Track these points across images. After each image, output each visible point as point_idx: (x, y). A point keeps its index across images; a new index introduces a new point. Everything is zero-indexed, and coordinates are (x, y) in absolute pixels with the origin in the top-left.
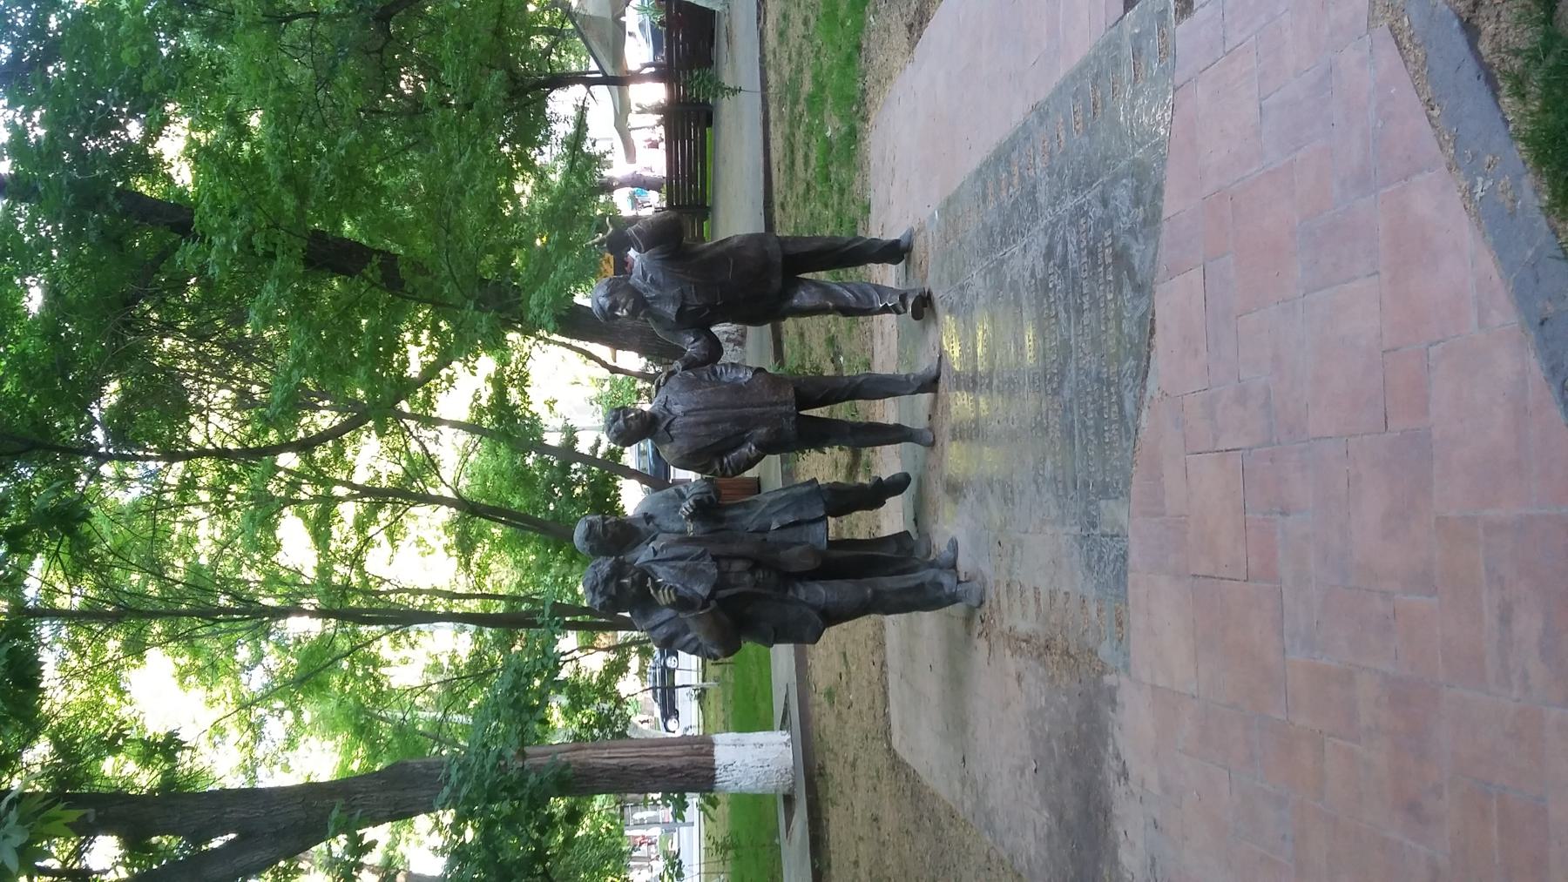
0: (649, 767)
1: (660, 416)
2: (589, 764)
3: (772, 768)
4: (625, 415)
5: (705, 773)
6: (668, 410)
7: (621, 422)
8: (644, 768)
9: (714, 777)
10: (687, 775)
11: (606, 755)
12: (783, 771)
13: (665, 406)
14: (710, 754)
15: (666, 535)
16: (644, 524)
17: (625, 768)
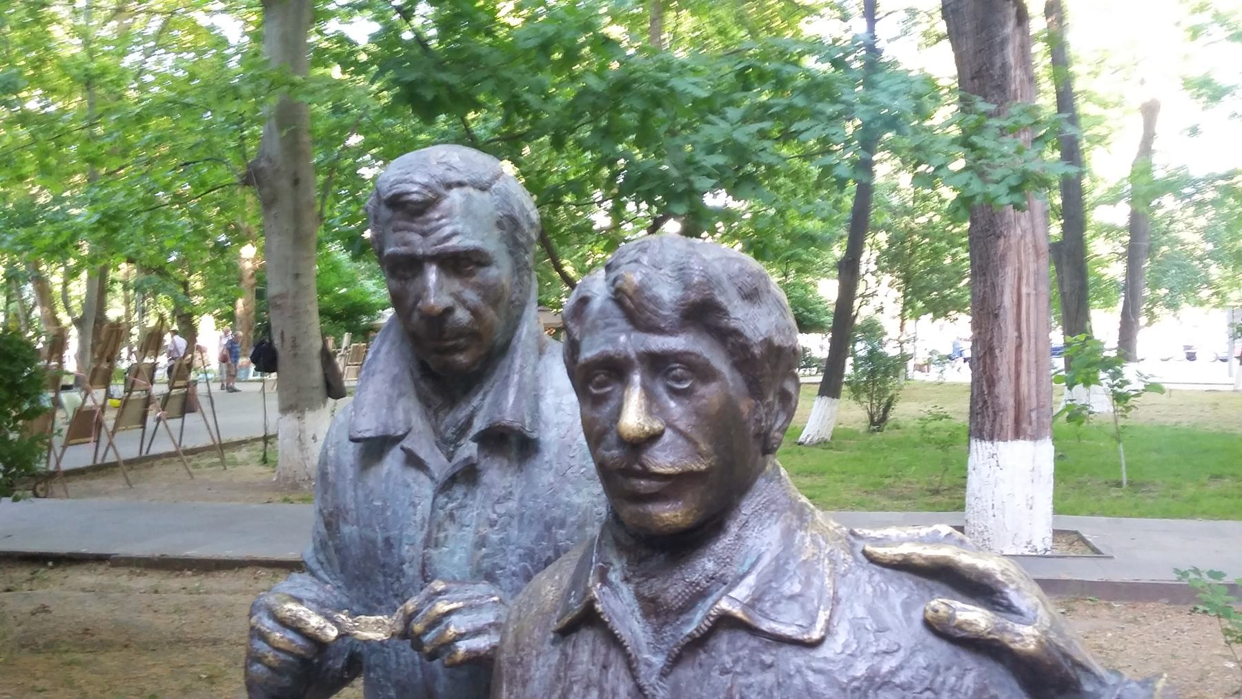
0: (997, 351)
1: (673, 588)
2: (1003, 268)
3: (991, 521)
4: (657, 364)
5: (987, 427)
6: (698, 643)
7: (627, 342)
8: (995, 344)
9: (982, 438)
10: (985, 402)
11: (1024, 290)
12: (986, 535)
13: (726, 622)
14: (1018, 434)
15: (425, 506)
16: (479, 425)
17: (996, 316)
